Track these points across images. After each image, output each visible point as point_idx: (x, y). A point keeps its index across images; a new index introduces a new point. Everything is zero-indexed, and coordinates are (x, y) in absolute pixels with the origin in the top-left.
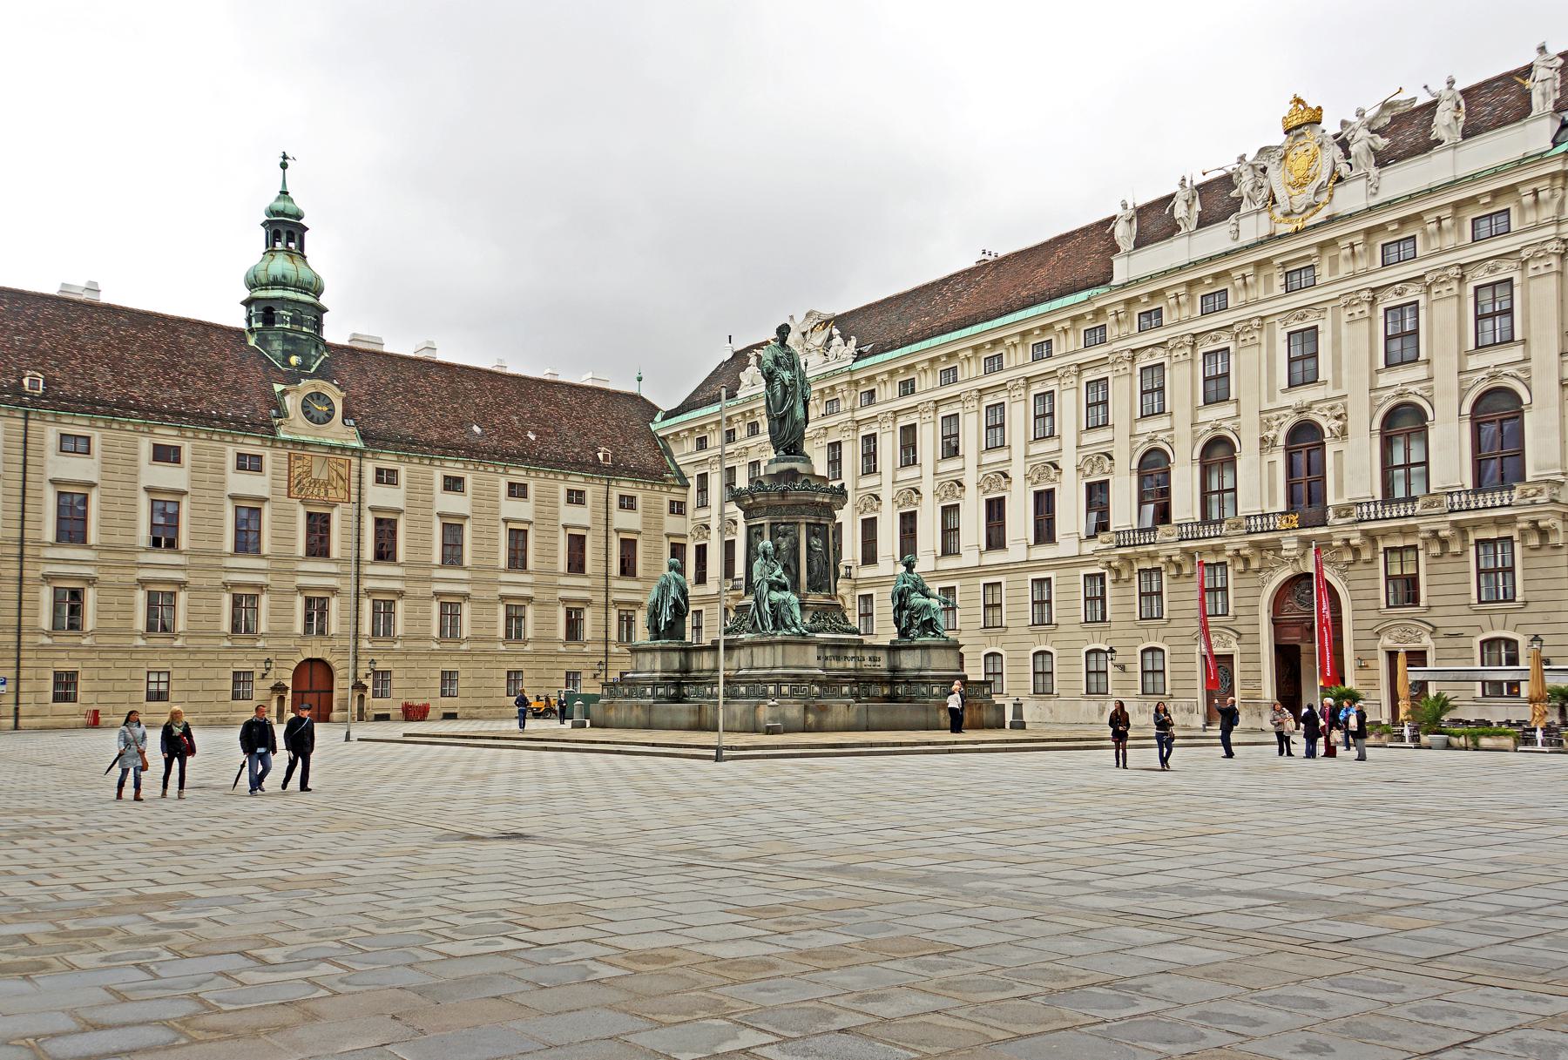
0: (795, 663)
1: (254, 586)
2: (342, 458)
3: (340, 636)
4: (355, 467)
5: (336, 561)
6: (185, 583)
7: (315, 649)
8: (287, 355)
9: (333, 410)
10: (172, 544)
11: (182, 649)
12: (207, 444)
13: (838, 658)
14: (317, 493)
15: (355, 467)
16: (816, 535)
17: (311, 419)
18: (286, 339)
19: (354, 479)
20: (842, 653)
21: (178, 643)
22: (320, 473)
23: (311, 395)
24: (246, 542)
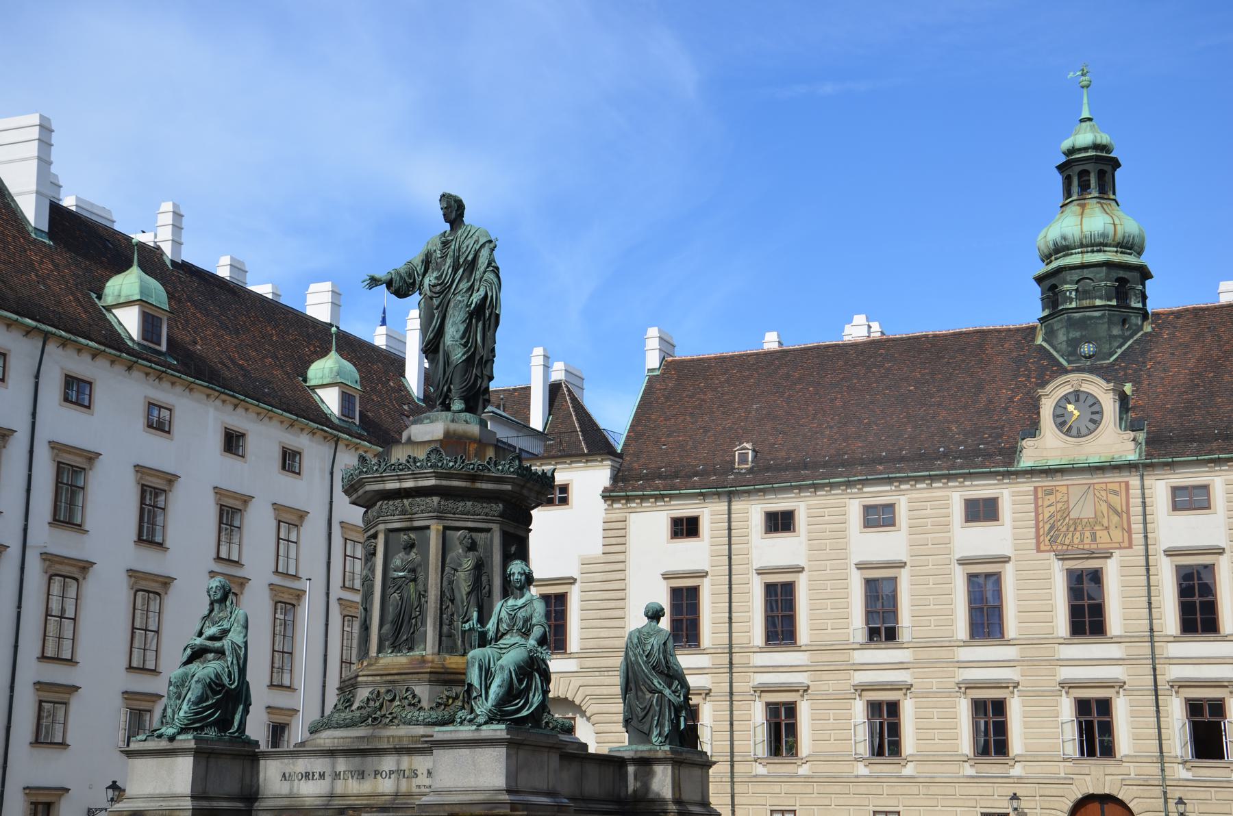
0: (149, 789)
1: (998, 685)
2: (1114, 480)
3: (1133, 759)
4: (1135, 492)
5: (1117, 641)
6: (909, 687)
7: (1097, 777)
8: (1074, 344)
9: (1100, 412)
10: (891, 635)
11: (911, 779)
12: (926, 494)
13: (361, 775)
14: (1075, 540)
15: (1135, 492)
16: (410, 546)
17: (1068, 433)
18: (1072, 324)
19: (1136, 510)
20: (371, 762)
21: (909, 770)
22: (1084, 510)
23: (1066, 399)
24: (986, 619)
